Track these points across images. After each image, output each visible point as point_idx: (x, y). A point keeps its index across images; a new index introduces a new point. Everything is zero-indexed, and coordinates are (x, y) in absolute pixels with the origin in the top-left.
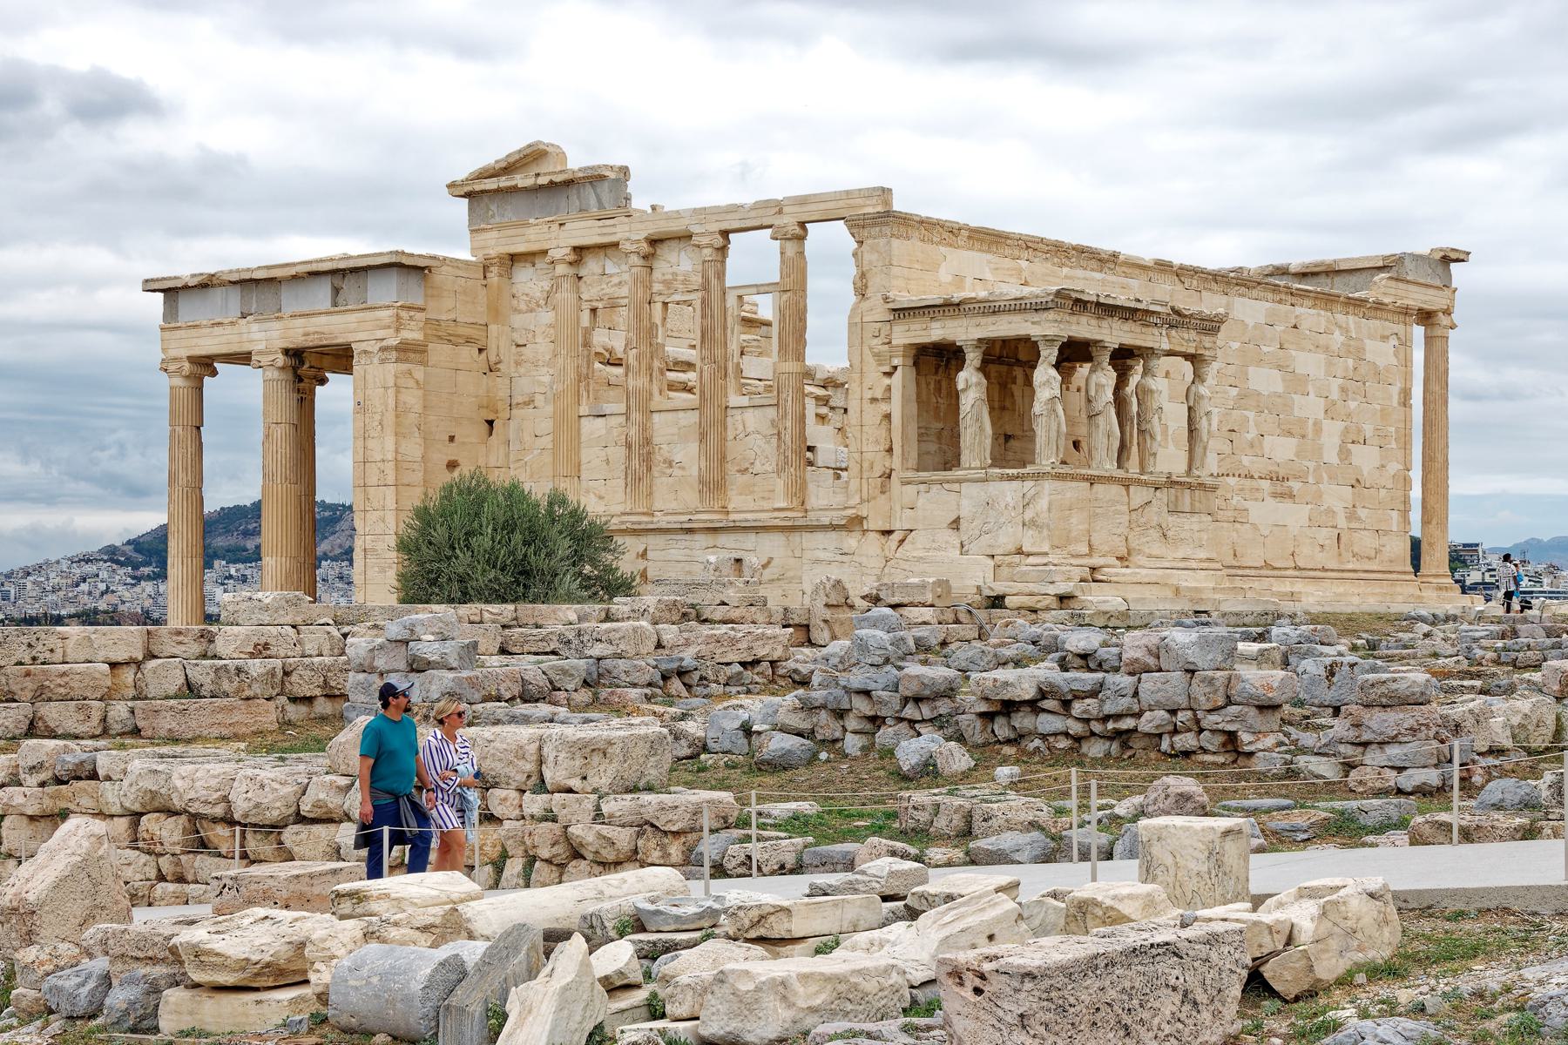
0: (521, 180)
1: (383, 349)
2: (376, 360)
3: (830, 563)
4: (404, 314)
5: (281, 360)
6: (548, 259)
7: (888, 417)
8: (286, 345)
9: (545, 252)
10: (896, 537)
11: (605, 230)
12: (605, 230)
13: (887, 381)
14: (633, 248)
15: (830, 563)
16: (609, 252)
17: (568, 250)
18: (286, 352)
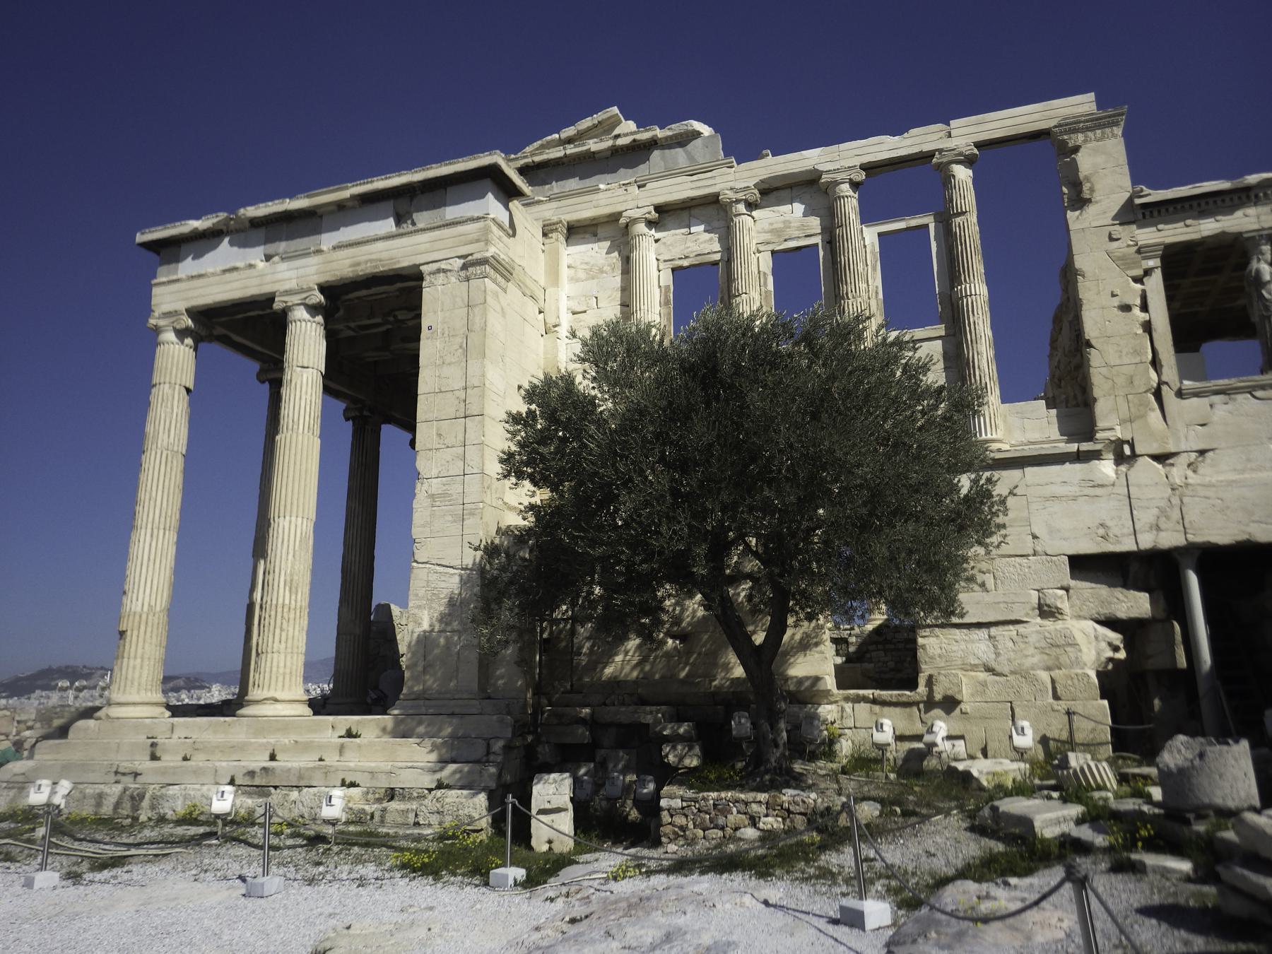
0: (594, 145)
1: (465, 267)
2: (453, 279)
3: (1075, 499)
4: (495, 229)
5: (318, 298)
6: (622, 221)
7: (1148, 327)
8: (322, 279)
9: (614, 218)
10: (1182, 460)
11: (699, 184)
12: (699, 184)
13: (1138, 286)
14: (740, 196)
15: (1075, 499)
16: (695, 212)
17: (652, 208)
18: (323, 288)
